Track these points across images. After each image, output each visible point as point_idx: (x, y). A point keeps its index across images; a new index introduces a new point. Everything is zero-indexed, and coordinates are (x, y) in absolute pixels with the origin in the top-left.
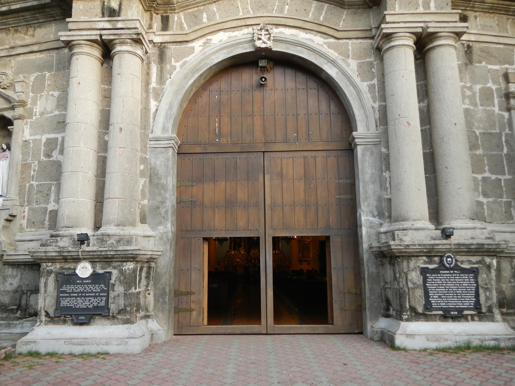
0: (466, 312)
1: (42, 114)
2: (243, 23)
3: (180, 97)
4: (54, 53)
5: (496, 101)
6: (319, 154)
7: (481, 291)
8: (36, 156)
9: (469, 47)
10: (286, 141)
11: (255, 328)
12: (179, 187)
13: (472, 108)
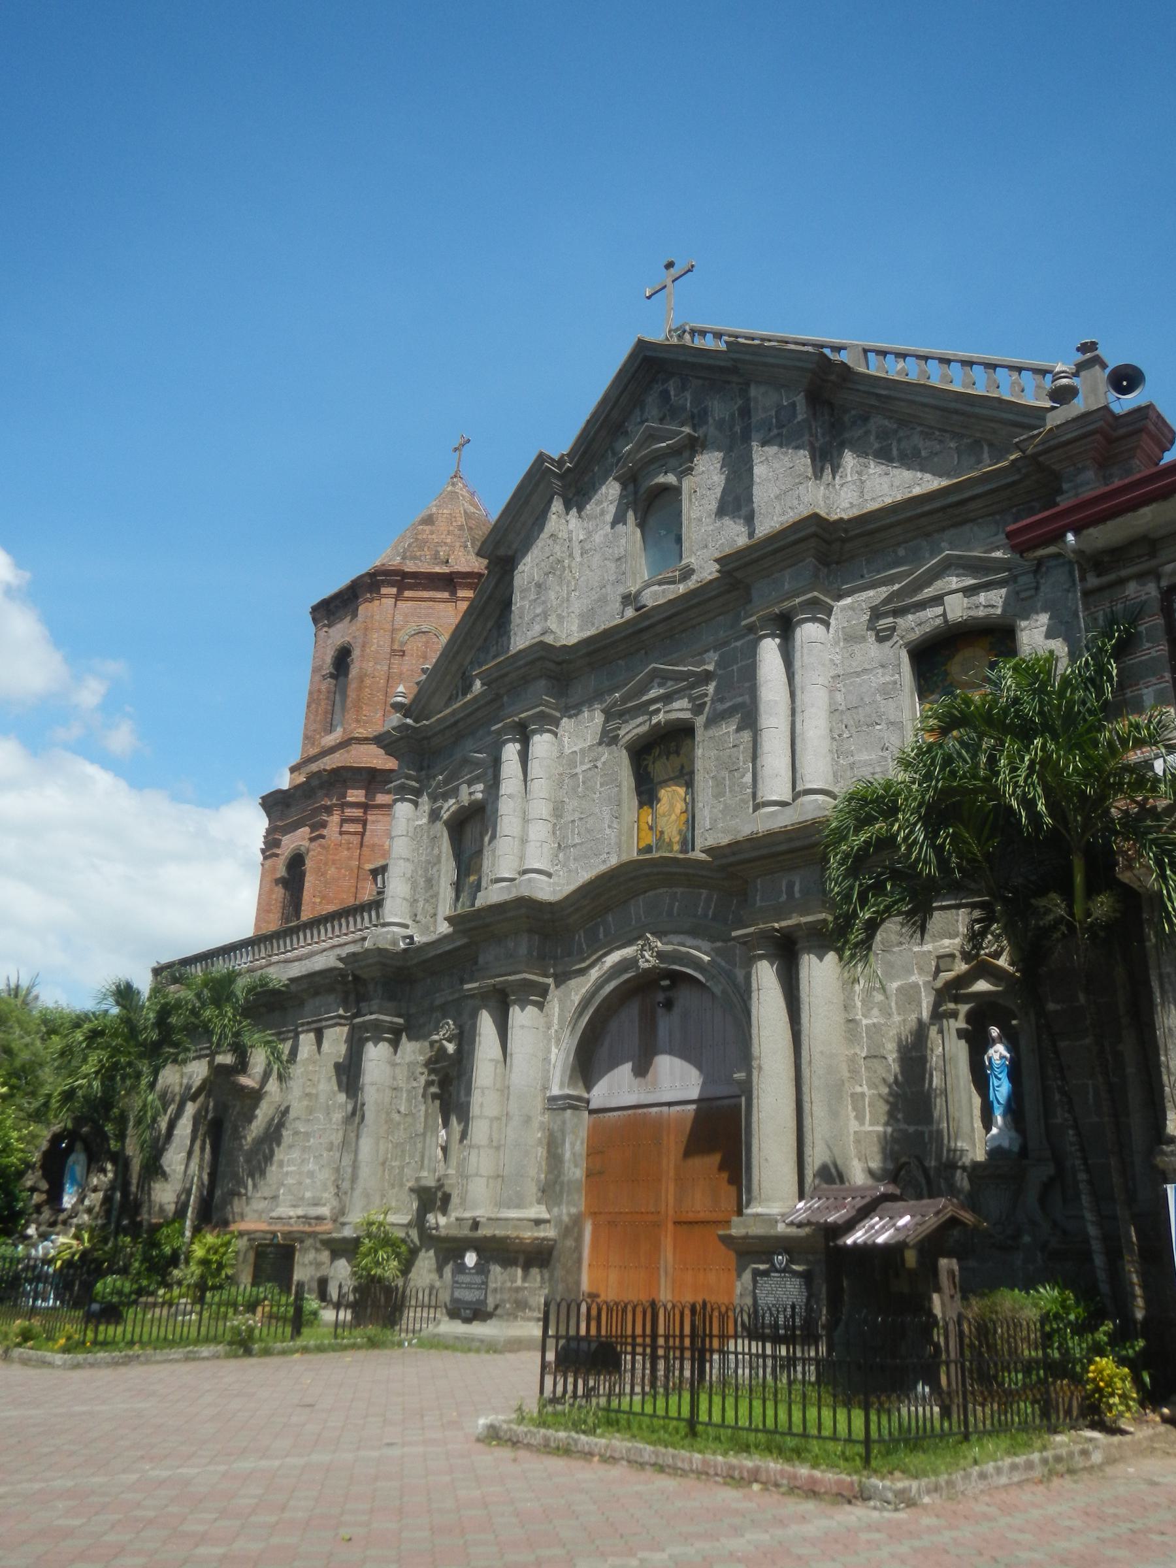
3: (576, 1042)
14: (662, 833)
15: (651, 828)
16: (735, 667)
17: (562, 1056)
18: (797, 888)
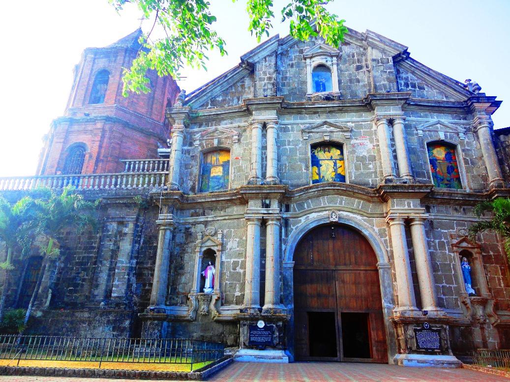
0: (436, 350)
1: (231, 249)
2: (322, 209)
3: (296, 243)
4: (236, 221)
5: (447, 248)
6: (362, 272)
7: (442, 341)
8: (228, 269)
9: (431, 221)
10: (345, 264)
11: (335, 359)
12: (294, 285)
13: (435, 251)
14: (323, 177)
15: (317, 174)
16: (362, 130)
17: (288, 247)
18: (412, 205)
